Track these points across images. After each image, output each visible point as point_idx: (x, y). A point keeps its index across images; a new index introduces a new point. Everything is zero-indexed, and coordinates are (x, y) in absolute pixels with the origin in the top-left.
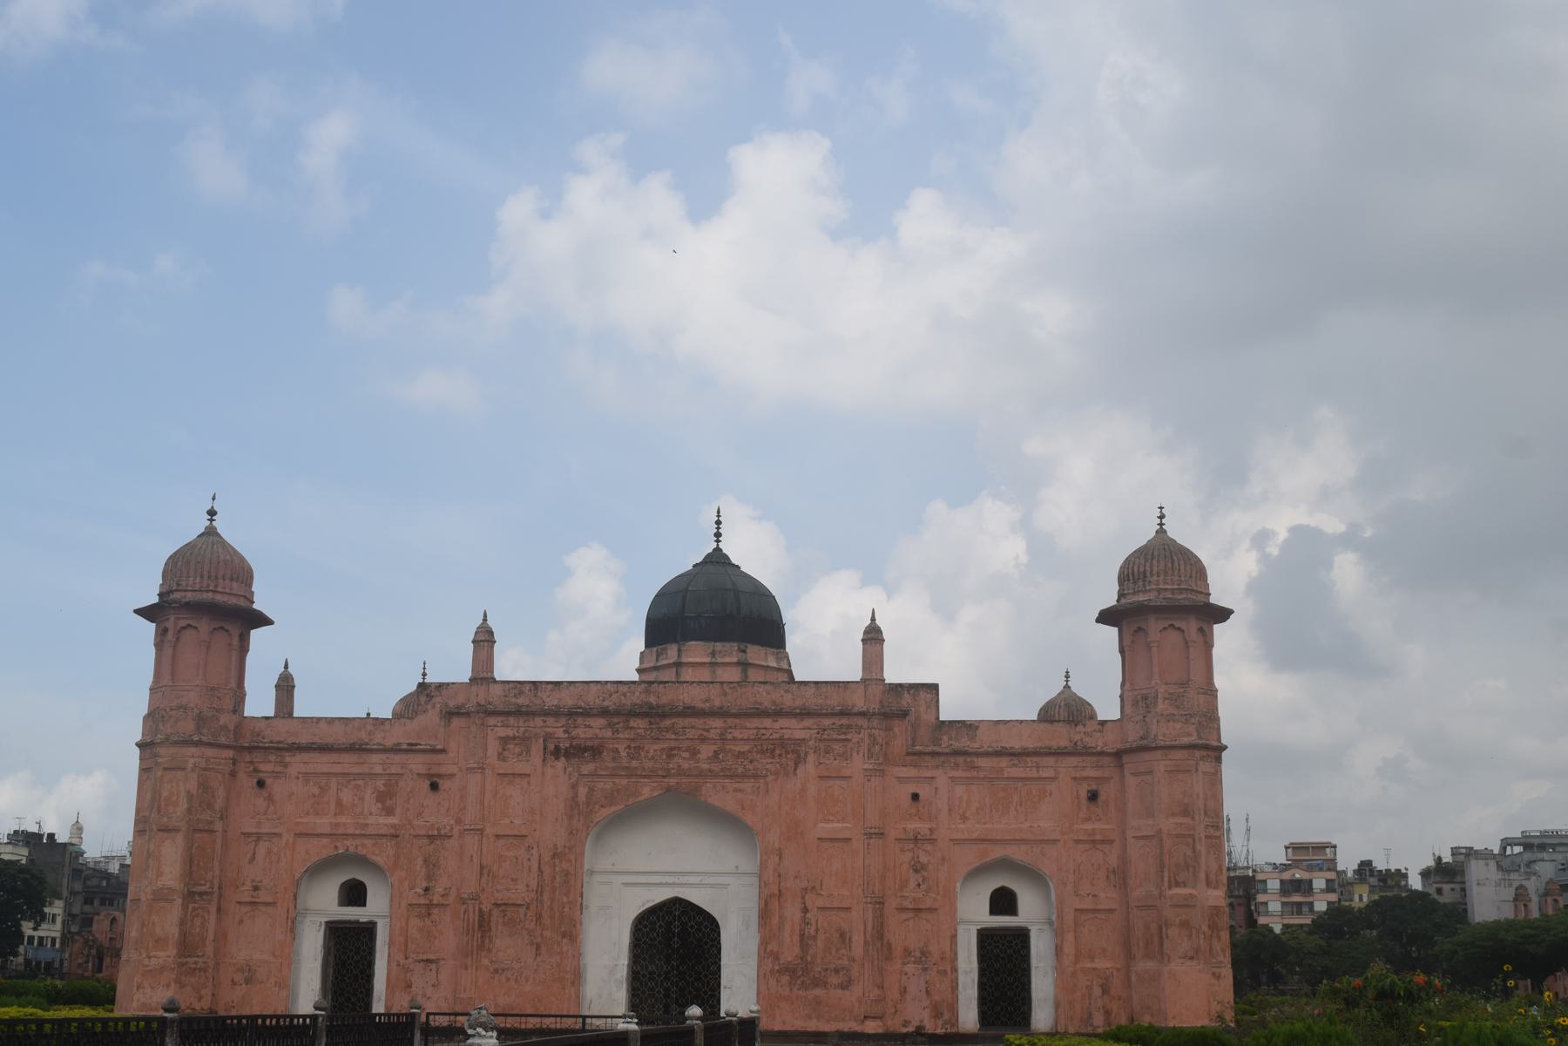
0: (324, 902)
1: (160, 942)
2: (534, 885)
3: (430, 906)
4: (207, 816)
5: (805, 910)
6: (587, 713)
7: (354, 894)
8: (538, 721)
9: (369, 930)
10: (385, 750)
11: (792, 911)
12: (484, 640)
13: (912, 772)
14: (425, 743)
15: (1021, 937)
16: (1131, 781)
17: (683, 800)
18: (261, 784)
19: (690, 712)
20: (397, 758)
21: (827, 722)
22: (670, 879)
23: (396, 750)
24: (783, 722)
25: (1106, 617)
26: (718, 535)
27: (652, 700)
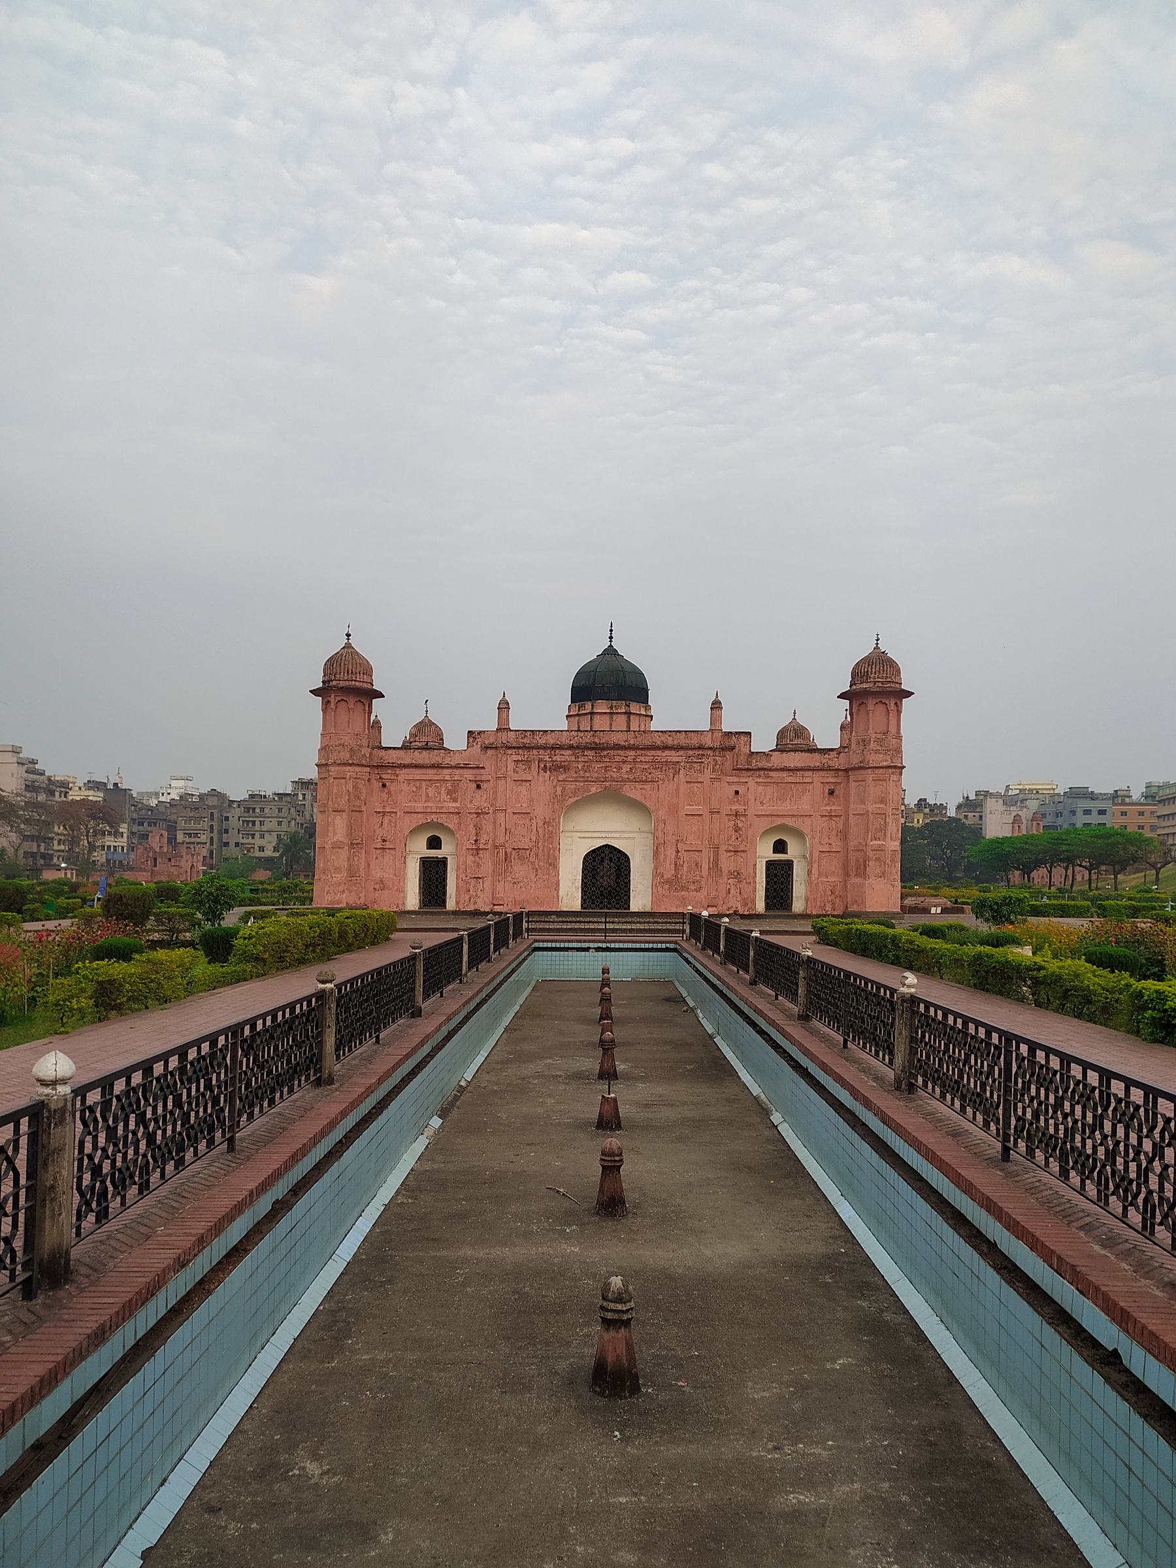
0: (419, 848)
1: (337, 869)
2: (534, 839)
3: (478, 849)
4: (357, 803)
5: (678, 852)
6: (561, 748)
7: (434, 843)
8: (535, 752)
9: (443, 862)
10: (451, 767)
11: (671, 852)
12: (504, 707)
13: (736, 779)
14: (473, 764)
15: (789, 864)
16: (852, 784)
17: (613, 796)
18: (384, 785)
19: (617, 747)
20: (458, 771)
21: (691, 753)
22: (604, 835)
23: (457, 767)
24: (667, 753)
26: (611, 638)
27: (597, 740)
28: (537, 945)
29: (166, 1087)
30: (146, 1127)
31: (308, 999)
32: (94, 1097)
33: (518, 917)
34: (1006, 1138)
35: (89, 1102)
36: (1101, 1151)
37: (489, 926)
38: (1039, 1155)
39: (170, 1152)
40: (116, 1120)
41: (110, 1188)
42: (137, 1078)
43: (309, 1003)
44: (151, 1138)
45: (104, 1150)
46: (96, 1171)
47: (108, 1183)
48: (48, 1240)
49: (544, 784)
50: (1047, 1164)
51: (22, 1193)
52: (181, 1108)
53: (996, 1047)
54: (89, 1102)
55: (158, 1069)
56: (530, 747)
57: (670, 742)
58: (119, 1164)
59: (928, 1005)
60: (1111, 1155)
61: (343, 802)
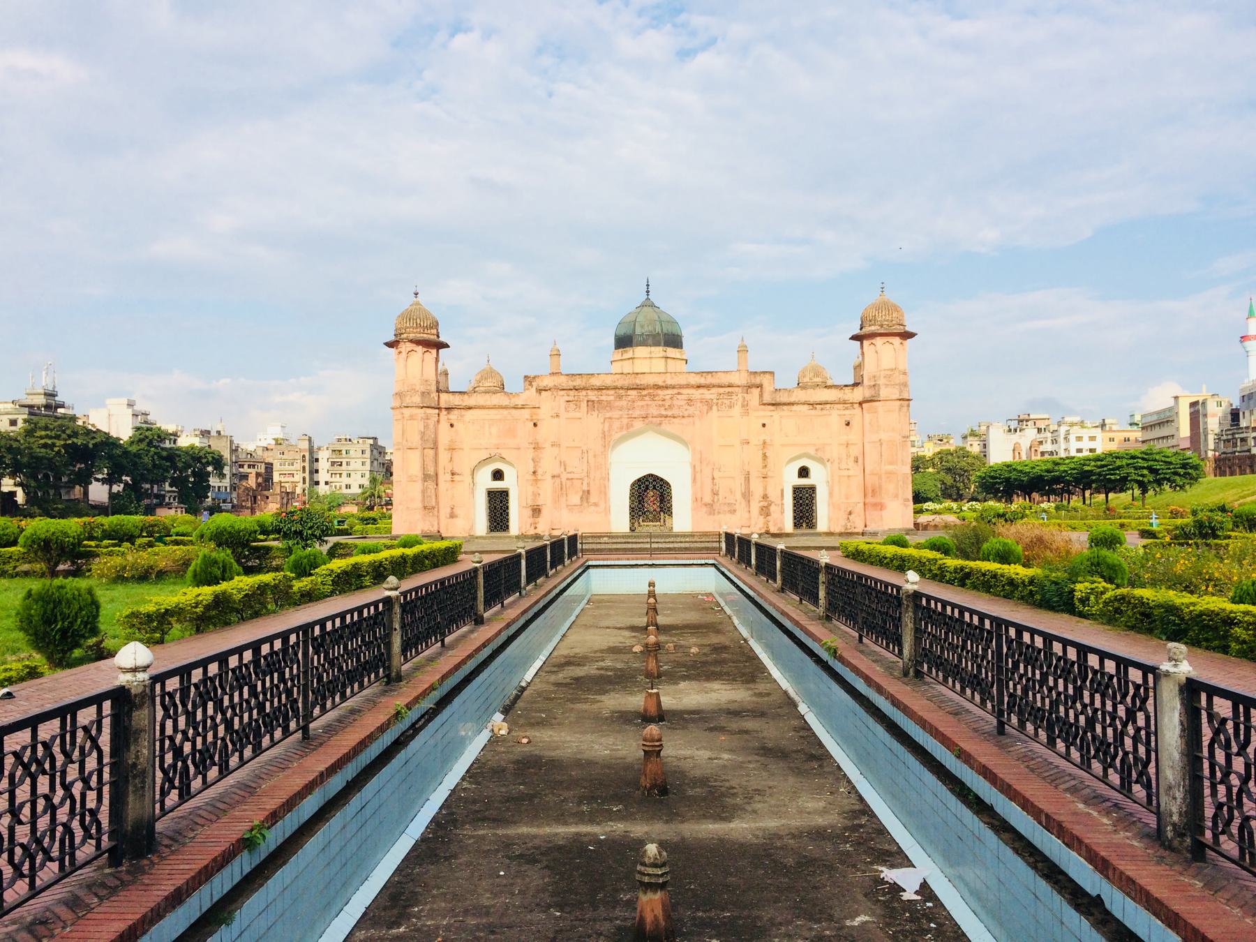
3: (536, 480)
6: (607, 388)
8: (584, 393)
13: (762, 413)
15: (812, 489)
16: (867, 416)
18: (452, 425)
21: (721, 390)
24: (701, 391)
25: (854, 338)
28: (590, 563)
29: (241, 679)
30: (224, 713)
31: (376, 604)
32: (173, 684)
33: (573, 539)
34: (1001, 713)
35: (169, 688)
36: (1082, 718)
37: (545, 546)
38: (1030, 727)
39: (248, 738)
40: (195, 706)
41: (192, 769)
42: (213, 669)
43: (376, 608)
44: (229, 724)
45: (184, 733)
46: (178, 752)
47: (189, 762)
48: (134, 809)
49: (594, 422)
50: (1036, 734)
51: (107, 770)
52: (257, 698)
53: (988, 632)
54: (169, 688)
55: (233, 662)
56: (582, 390)
57: (702, 381)
58: (199, 746)
59: (929, 598)
60: (1091, 722)
61: (416, 440)
